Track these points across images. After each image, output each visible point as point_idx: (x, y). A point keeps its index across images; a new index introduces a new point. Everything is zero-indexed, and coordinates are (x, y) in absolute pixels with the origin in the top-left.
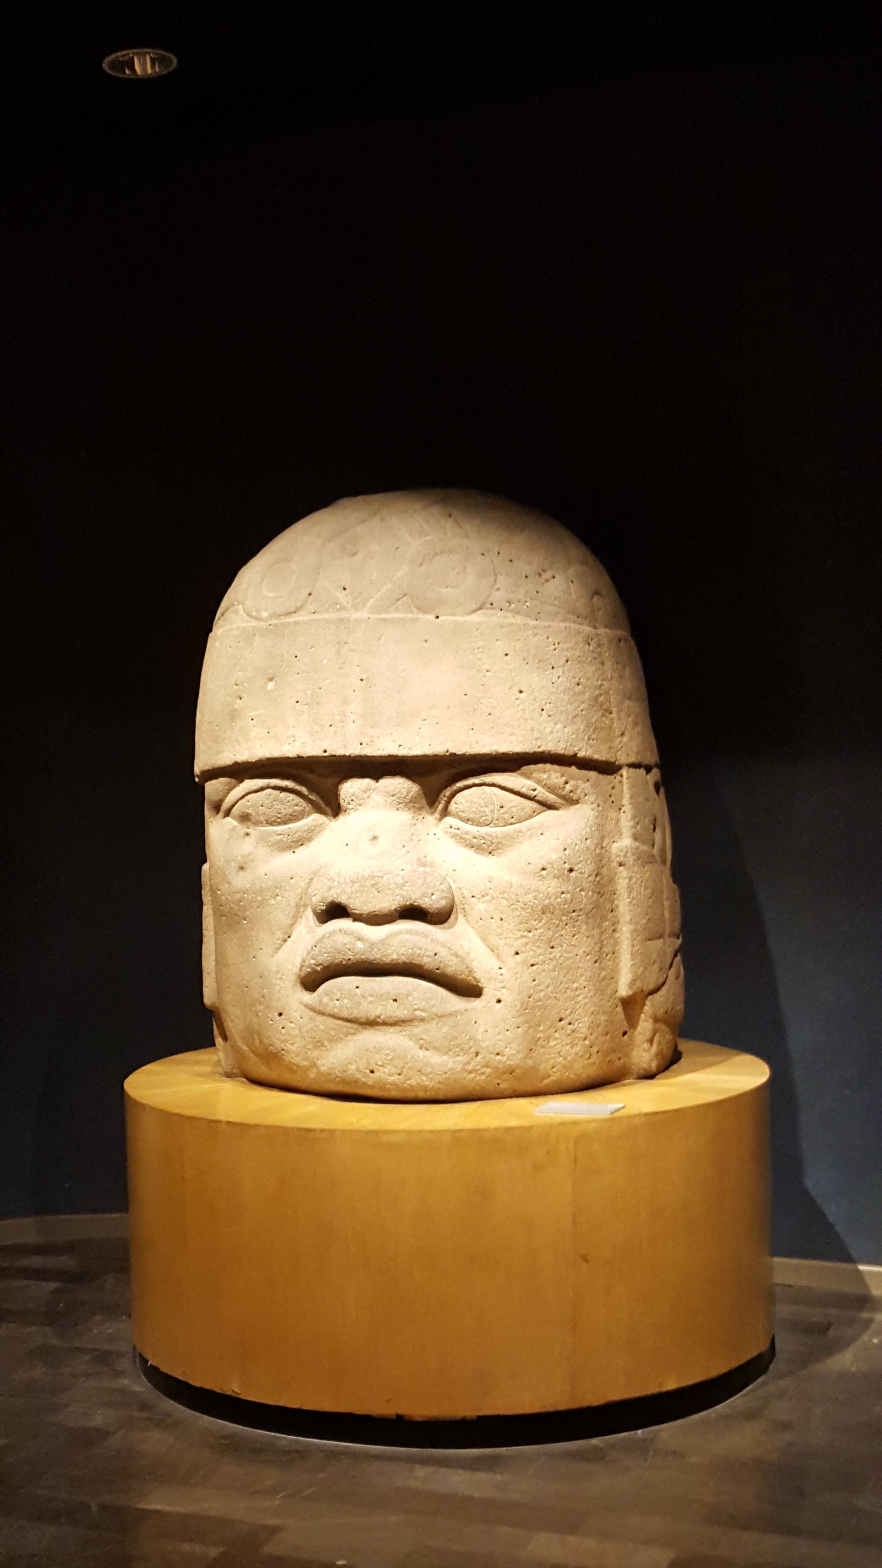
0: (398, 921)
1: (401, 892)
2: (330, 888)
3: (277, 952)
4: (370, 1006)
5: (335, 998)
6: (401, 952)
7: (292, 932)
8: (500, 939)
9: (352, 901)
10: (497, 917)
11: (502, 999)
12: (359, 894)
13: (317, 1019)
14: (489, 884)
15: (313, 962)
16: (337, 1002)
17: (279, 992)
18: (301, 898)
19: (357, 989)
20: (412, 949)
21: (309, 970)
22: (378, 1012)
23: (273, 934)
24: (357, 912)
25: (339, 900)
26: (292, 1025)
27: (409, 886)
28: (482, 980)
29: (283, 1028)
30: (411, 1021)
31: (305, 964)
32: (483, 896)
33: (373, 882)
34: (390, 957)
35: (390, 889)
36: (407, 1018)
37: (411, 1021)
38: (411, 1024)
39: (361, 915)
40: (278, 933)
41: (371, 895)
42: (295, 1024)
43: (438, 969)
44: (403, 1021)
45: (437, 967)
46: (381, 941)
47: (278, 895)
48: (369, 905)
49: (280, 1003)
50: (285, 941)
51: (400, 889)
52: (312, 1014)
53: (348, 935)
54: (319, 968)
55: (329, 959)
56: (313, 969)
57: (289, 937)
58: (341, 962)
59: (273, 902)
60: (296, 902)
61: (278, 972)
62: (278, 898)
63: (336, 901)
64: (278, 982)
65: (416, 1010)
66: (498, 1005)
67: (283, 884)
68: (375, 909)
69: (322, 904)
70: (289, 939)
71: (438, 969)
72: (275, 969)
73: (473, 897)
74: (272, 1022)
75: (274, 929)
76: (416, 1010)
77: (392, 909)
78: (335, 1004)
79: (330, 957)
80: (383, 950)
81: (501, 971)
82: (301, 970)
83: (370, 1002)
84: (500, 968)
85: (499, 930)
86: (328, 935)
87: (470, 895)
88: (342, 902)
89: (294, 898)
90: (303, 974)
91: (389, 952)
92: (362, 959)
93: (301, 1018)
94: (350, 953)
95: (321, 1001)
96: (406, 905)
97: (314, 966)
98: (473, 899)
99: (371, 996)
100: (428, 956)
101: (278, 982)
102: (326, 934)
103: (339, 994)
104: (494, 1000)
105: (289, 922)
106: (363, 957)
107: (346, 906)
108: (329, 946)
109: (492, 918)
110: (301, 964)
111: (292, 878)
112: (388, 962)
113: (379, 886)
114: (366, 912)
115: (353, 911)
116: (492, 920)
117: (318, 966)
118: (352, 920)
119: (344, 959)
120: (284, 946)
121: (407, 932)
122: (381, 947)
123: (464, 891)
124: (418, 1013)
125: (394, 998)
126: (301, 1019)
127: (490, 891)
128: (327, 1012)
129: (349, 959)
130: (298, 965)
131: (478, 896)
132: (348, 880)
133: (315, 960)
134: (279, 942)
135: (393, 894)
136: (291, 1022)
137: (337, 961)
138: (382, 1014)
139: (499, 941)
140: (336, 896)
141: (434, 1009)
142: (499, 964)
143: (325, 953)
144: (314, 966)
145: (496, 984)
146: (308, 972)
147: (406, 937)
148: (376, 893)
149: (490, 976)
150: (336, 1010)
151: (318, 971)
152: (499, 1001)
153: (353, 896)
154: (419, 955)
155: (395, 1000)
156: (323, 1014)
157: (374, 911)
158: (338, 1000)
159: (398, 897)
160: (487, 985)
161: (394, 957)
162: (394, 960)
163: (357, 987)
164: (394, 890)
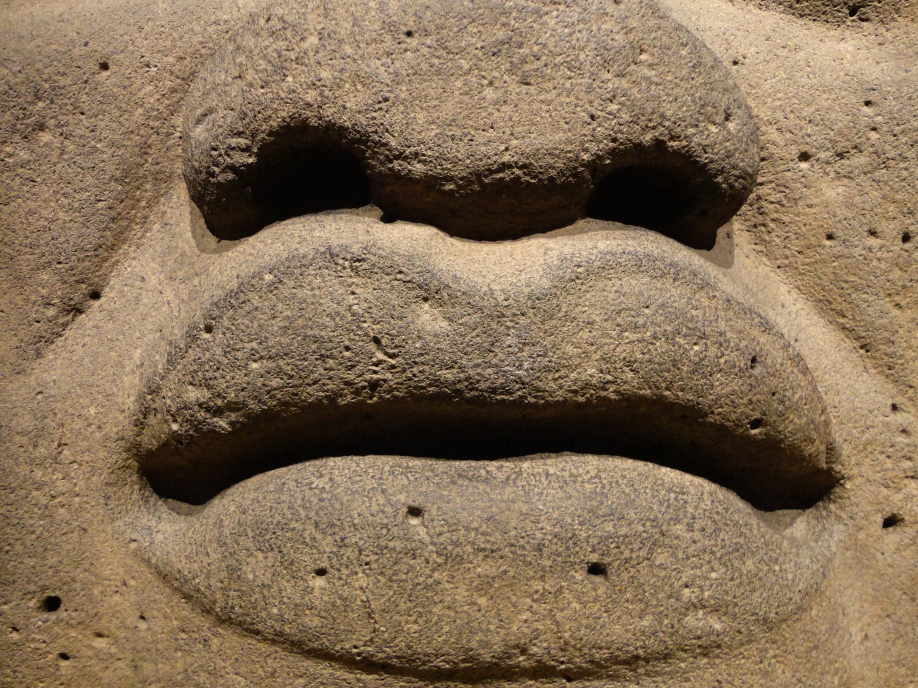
0: (581, 223)
1: (624, 83)
2: (281, 71)
3: (39, 354)
4: (482, 601)
5: (307, 560)
6: (623, 351)
7: (105, 278)
8: (898, 305)
9: (395, 117)
10: (891, 229)
11: (904, 513)
12: (433, 87)
13: (215, 641)
14: (866, 109)
15: (193, 394)
16: (320, 582)
17: (47, 514)
18: (144, 149)
19: (414, 521)
20: (669, 338)
21: (175, 427)
22: (518, 628)
23: (20, 282)
24: (418, 168)
25: (329, 112)
26: (100, 643)
27: (651, 66)
28: (845, 450)
29: (64, 656)
30: (666, 657)
31: (158, 404)
32: (841, 155)
33: (501, 34)
34: (573, 376)
35: (574, 67)
36: (653, 645)
37: (666, 657)
38: (661, 666)
39: (431, 182)
40: (45, 276)
41: (489, 93)
42: (116, 641)
43: (756, 424)
44: (632, 661)
45: (757, 415)
46: (536, 299)
47: (42, 127)
48: (480, 137)
49: (52, 560)
50: (78, 310)
51: (621, 75)
52: (186, 610)
53: (370, 273)
54: (222, 423)
55: (275, 382)
56: (197, 425)
57: (96, 295)
58: (333, 398)
59: (24, 155)
60: (123, 161)
61: (37, 436)
62: (45, 137)
63: (314, 122)
64: (39, 474)
65: (693, 606)
66: (893, 537)
67: (63, 81)
68: (506, 158)
69: (243, 141)
70: (97, 303)
71: (756, 424)
72: (26, 422)
73: (804, 157)
74: (15, 636)
75: (27, 260)
76: (693, 606)
77: (586, 157)
78: (309, 590)
79: (280, 372)
80: (548, 341)
81: (899, 418)
82: (140, 425)
83: (485, 585)
84: (894, 408)
85: (896, 274)
86: (268, 278)
87: (795, 151)
88: (345, 120)
89: (112, 144)
90: (149, 442)
91: (570, 349)
92: (436, 382)
93: (142, 618)
94: (380, 356)
95: (233, 572)
96: (638, 146)
97: (201, 415)
98: (804, 165)
99: (489, 553)
100: (730, 370)
101: (39, 474)
102: (259, 275)
103: (327, 544)
104: (879, 519)
105: (92, 236)
106: (448, 375)
107: (364, 139)
108: (277, 324)
109: (873, 233)
110: (141, 398)
111: (105, 67)
112: (559, 396)
113: (525, 51)
114: (459, 172)
115: (396, 165)
116: (872, 242)
117: (218, 412)
118: (380, 212)
119: (348, 383)
120: (67, 333)
121: (642, 264)
122: (535, 333)
123: (773, 134)
124: (696, 621)
125: (594, 558)
126: (143, 625)
127: (873, 135)
128: (268, 626)
129: (374, 386)
130: (130, 403)
131: (823, 155)
132: (372, 25)
133: (209, 387)
134: (51, 312)
135: (589, 90)
136: (99, 635)
137: (313, 393)
138: (537, 634)
139: (896, 312)
140: (311, 96)
141: (756, 597)
142: (885, 394)
143: (254, 356)
144: (201, 415)
145: (889, 464)
146: (175, 436)
147: (637, 284)
148: (514, 88)
149: (867, 436)
150: (312, 621)
151: (213, 433)
152: (890, 522)
153: (403, 92)
154: (697, 367)
155: (596, 569)
156: (250, 630)
157: (504, 167)
158: (321, 572)
159: (613, 107)
160: (855, 471)
161: (591, 372)
162: (587, 385)
163: (415, 512)
164: (594, 76)
